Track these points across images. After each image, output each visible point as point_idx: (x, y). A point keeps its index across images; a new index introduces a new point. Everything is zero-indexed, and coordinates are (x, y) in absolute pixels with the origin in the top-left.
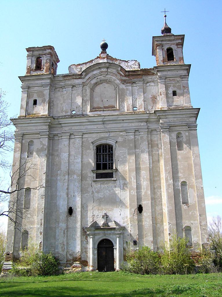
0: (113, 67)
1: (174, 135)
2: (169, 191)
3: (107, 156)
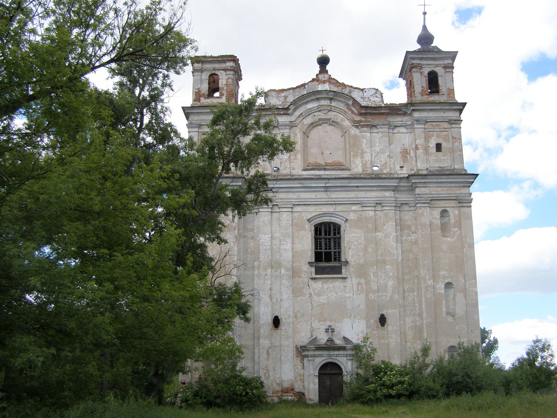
0: (340, 99)
1: (437, 213)
2: (428, 296)
3: (332, 241)
